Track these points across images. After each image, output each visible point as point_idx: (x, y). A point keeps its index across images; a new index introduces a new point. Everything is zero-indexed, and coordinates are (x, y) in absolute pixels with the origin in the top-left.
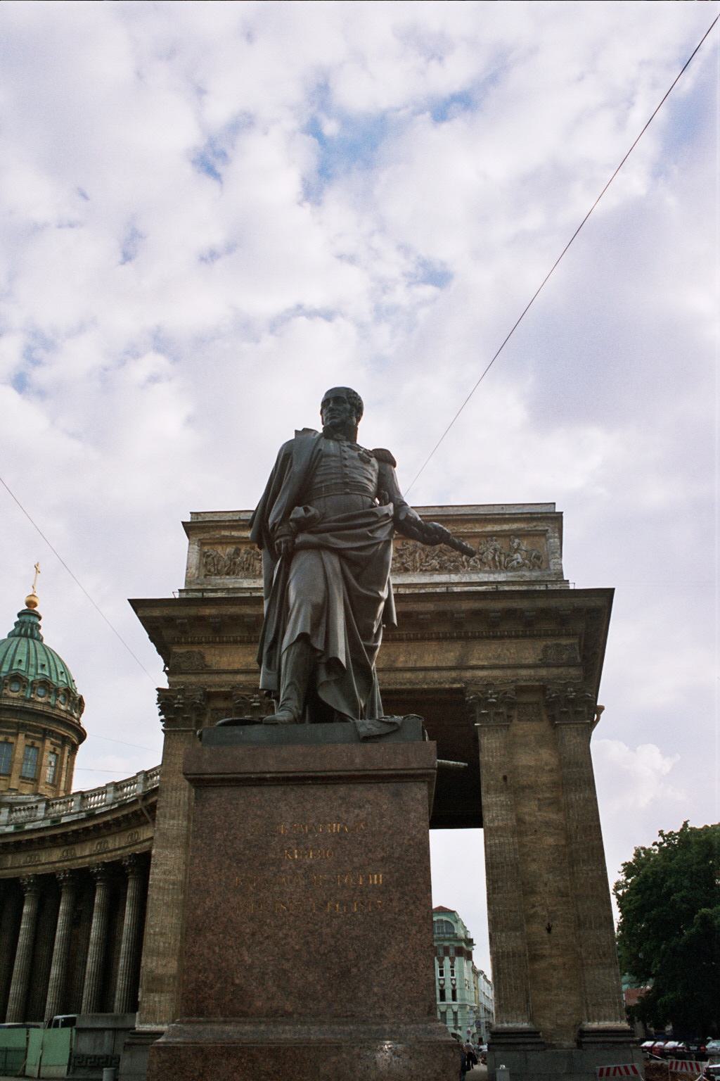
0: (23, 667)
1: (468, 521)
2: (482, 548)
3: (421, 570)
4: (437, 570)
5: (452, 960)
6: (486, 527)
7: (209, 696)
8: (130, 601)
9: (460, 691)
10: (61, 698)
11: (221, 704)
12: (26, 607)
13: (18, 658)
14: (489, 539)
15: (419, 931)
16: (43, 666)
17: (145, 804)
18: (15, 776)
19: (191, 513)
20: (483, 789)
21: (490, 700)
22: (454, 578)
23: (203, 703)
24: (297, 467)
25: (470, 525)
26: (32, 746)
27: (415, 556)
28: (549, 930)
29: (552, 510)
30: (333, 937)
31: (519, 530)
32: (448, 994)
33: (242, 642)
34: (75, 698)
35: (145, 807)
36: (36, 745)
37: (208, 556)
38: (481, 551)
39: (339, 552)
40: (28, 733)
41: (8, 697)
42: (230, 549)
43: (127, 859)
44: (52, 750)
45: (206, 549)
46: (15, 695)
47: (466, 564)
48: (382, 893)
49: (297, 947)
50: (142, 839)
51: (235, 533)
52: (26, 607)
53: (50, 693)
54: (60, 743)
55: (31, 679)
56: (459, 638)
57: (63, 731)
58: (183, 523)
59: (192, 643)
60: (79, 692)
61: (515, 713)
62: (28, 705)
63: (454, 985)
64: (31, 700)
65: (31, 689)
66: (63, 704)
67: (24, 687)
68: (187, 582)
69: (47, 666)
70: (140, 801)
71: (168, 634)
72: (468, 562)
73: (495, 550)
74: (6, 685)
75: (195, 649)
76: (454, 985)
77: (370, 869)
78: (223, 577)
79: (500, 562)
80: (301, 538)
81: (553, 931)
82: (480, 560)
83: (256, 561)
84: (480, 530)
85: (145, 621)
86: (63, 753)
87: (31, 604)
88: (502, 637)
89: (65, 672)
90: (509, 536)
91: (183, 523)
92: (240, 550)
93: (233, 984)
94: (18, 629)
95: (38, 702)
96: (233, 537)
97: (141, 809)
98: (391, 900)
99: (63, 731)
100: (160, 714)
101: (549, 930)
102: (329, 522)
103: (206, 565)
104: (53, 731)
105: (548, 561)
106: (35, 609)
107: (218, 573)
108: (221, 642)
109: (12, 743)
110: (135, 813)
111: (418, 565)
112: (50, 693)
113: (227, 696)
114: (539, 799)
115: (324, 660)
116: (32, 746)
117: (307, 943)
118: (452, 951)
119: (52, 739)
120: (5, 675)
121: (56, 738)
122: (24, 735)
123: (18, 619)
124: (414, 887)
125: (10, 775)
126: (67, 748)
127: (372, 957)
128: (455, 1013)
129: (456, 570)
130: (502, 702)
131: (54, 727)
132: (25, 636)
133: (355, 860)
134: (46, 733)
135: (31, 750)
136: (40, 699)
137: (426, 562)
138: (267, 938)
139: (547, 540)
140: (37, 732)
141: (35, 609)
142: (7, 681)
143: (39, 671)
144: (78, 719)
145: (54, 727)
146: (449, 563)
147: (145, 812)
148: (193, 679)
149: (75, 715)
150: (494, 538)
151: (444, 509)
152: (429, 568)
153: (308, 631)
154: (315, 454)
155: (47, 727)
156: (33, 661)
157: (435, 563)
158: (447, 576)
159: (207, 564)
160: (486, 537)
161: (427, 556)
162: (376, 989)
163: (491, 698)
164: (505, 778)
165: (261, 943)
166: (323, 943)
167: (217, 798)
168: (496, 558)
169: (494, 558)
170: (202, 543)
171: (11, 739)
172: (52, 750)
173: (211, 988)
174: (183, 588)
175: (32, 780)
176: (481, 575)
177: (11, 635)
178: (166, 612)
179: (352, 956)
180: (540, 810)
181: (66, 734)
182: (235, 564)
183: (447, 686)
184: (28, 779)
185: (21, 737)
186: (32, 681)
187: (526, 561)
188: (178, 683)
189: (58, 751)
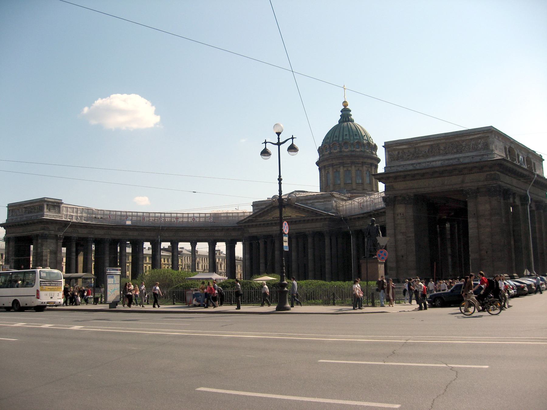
0: (348, 137)
1: (464, 136)
6: (469, 137)
10: (366, 147)
12: (343, 107)
13: (345, 133)
16: (356, 135)
18: (354, 184)
20: (469, 217)
22: (461, 155)
25: (465, 137)
26: (358, 170)
28: (487, 253)
31: (480, 137)
33: (402, 181)
34: (372, 145)
36: (360, 169)
38: (469, 145)
40: (356, 165)
41: (344, 152)
42: (396, 152)
44: (367, 170)
45: (390, 153)
46: (346, 150)
51: (397, 147)
52: (343, 107)
53: (361, 146)
54: (370, 166)
55: (352, 142)
56: (461, 175)
57: (370, 161)
59: (390, 183)
60: (374, 142)
62: (353, 153)
64: (353, 151)
65: (353, 146)
66: (368, 150)
67: (350, 146)
69: (358, 135)
72: (465, 149)
73: (473, 144)
74: (343, 146)
78: (396, 161)
79: (474, 148)
80: (369, 239)
81: (488, 253)
82: (469, 148)
84: (469, 138)
86: (372, 170)
87: (345, 104)
88: (473, 173)
89: (366, 135)
91: (383, 146)
92: (399, 152)
94: (342, 118)
95: (357, 151)
96: (397, 149)
99: (370, 161)
101: (487, 253)
103: (391, 158)
104: (365, 162)
105: (489, 147)
106: (347, 107)
107: (394, 160)
108: (397, 182)
109: (350, 170)
112: (361, 146)
113: (401, 196)
114: (485, 219)
116: (358, 170)
119: (366, 165)
120: (341, 142)
121: (368, 164)
122: (354, 166)
123: (341, 114)
125: (351, 183)
126: (373, 168)
129: (461, 152)
131: (365, 160)
132: (346, 121)
134: (363, 164)
135: (358, 172)
136: (358, 150)
137: (453, 150)
139: (489, 139)
140: (361, 164)
141: (347, 107)
142: (342, 145)
143: (355, 138)
144: (376, 154)
145: (365, 160)
149: (374, 152)
150: (473, 140)
152: (453, 152)
155: (363, 161)
156: (351, 134)
157: (455, 150)
158: (458, 155)
161: (453, 148)
163: (470, 192)
164: (474, 214)
168: (474, 146)
170: (388, 152)
171: (350, 169)
172: (367, 170)
174: (385, 166)
175: (361, 184)
176: (469, 153)
177: (340, 122)
178: (381, 176)
180: (485, 222)
181: (372, 162)
182: (398, 157)
183: (459, 189)
184: (359, 184)
185: (353, 167)
186: (353, 143)
187: (483, 147)
189: (370, 170)
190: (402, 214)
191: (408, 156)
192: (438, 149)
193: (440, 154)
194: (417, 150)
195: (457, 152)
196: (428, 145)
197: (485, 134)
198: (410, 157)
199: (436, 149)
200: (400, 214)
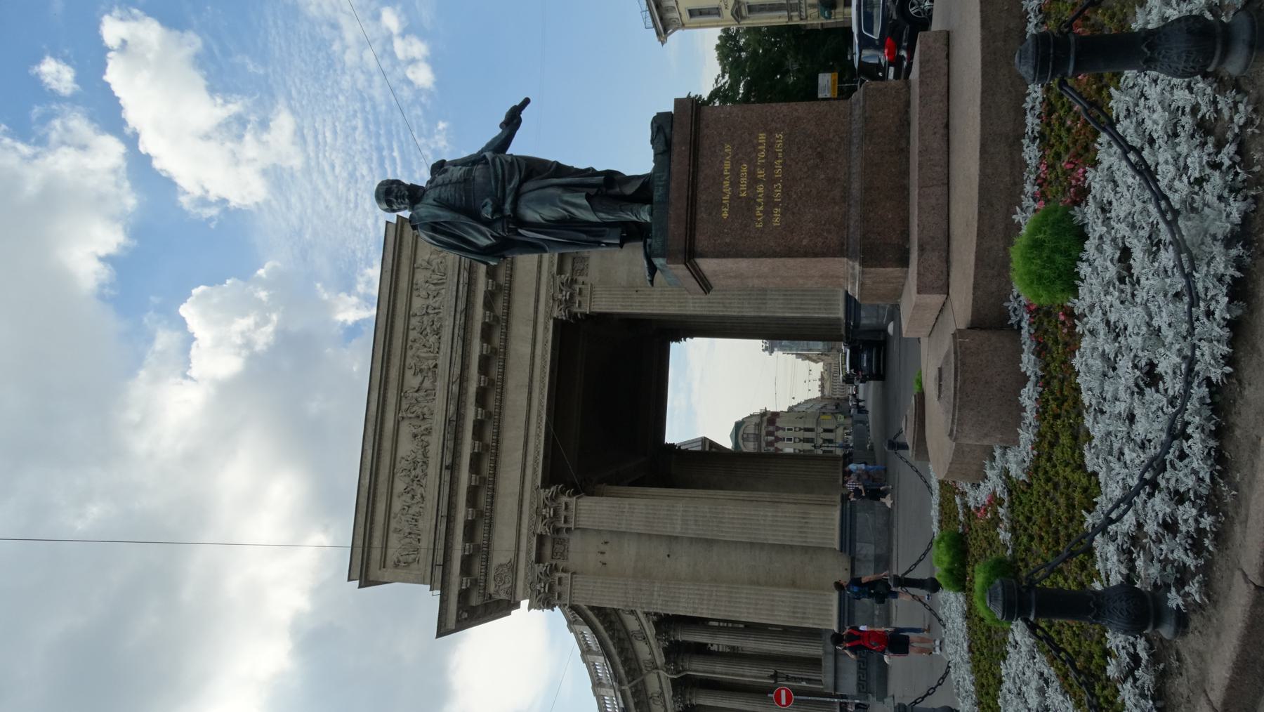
2: (424, 293)
3: (438, 352)
4: (440, 338)
5: (778, 429)
7: (539, 559)
8: (437, 638)
9: (556, 321)
11: (548, 550)
14: (414, 287)
15: (797, 110)
17: (626, 683)
19: (349, 579)
21: (568, 298)
23: (546, 564)
24: (445, 215)
27: (424, 358)
29: (394, 227)
30: (797, 163)
32: (809, 435)
35: (629, 682)
37: (399, 561)
39: (521, 182)
43: (677, 705)
45: (390, 563)
47: (436, 311)
48: (771, 133)
49: (803, 185)
50: (658, 689)
58: (360, 587)
61: (580, 279)
63: (800, 429)
68: (424, 583)
70: (623, 688)
71: (475, 600)
75: (492, 573)
76: (800, 429)
77: (755, 141)
80: (507, 207)
82: (434, 297)
83: (410, 512)
85: (462, 624)
90: (414, 268)
91: (360, 587)
93: (824, 225)
97: (631, 688)
98: (776, 128)
100: (553, 610)
102: (497, 189)
110: (633, 694)
111: (432, 355)
115: (604, 189)
117: (800, 179)
118: (771, 428)
124: (768, 114)
127: (811, 139)
128: (826, 431)
130: (570, 288)
133: (749, 150)
138: (797, 205)
146: (434, 326)
147: (635, 682)
148: (521, 574)
151: (379, 325)
152: (437, 345)
153: (584, 194)
154: (435, 203)
157: (432, 339)
159: (403, 569)
160: (412, 287)
162: (831, 136)
165: (799, 209)
166: (801, 170)
167: (702, 242)
168: (435, 281)
169: (434, 284)
173: (827, 238)
174: (429, 586)
179: (810, 151)
182: (410, 533)
188: (525, 589)
190: (603, 548)
191: (413, 497)
192: (417, 391)
193: (431, 393)
194: (404, 464)
195: (437, 332)
196: (397, 424)
197: (405, 243)
198: (419, 492)
199: (414, 401)
200: (602, 553)
